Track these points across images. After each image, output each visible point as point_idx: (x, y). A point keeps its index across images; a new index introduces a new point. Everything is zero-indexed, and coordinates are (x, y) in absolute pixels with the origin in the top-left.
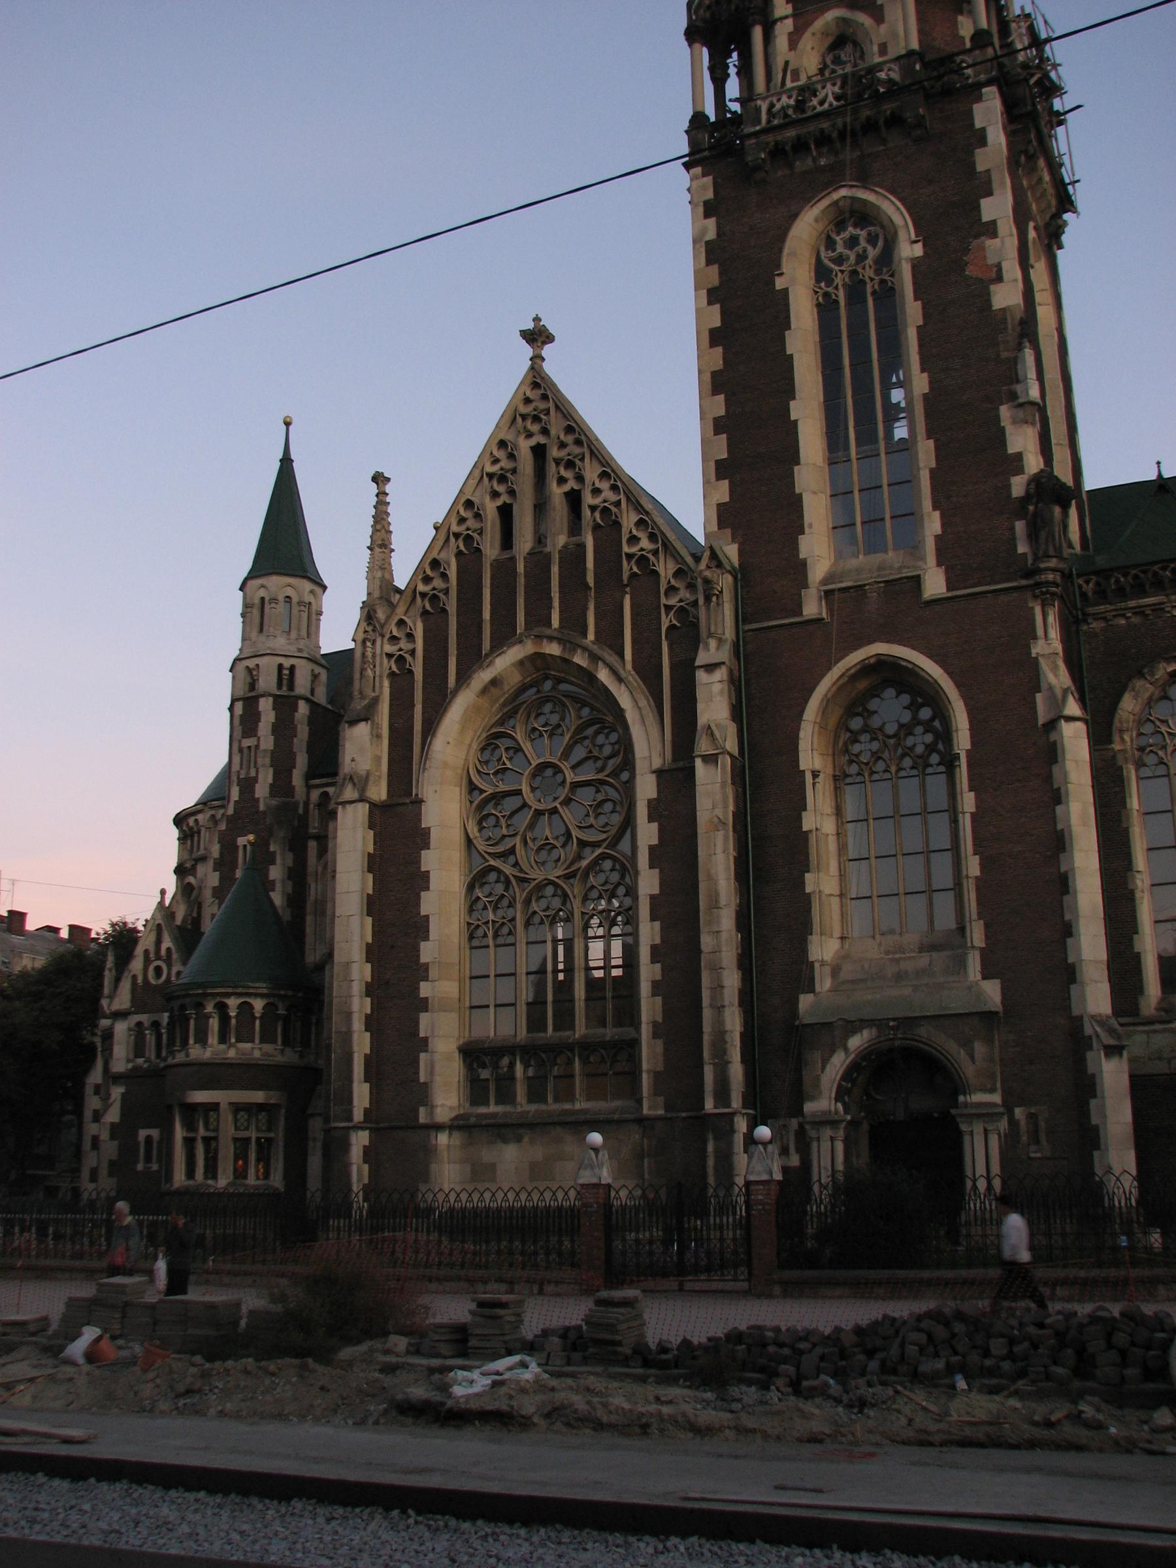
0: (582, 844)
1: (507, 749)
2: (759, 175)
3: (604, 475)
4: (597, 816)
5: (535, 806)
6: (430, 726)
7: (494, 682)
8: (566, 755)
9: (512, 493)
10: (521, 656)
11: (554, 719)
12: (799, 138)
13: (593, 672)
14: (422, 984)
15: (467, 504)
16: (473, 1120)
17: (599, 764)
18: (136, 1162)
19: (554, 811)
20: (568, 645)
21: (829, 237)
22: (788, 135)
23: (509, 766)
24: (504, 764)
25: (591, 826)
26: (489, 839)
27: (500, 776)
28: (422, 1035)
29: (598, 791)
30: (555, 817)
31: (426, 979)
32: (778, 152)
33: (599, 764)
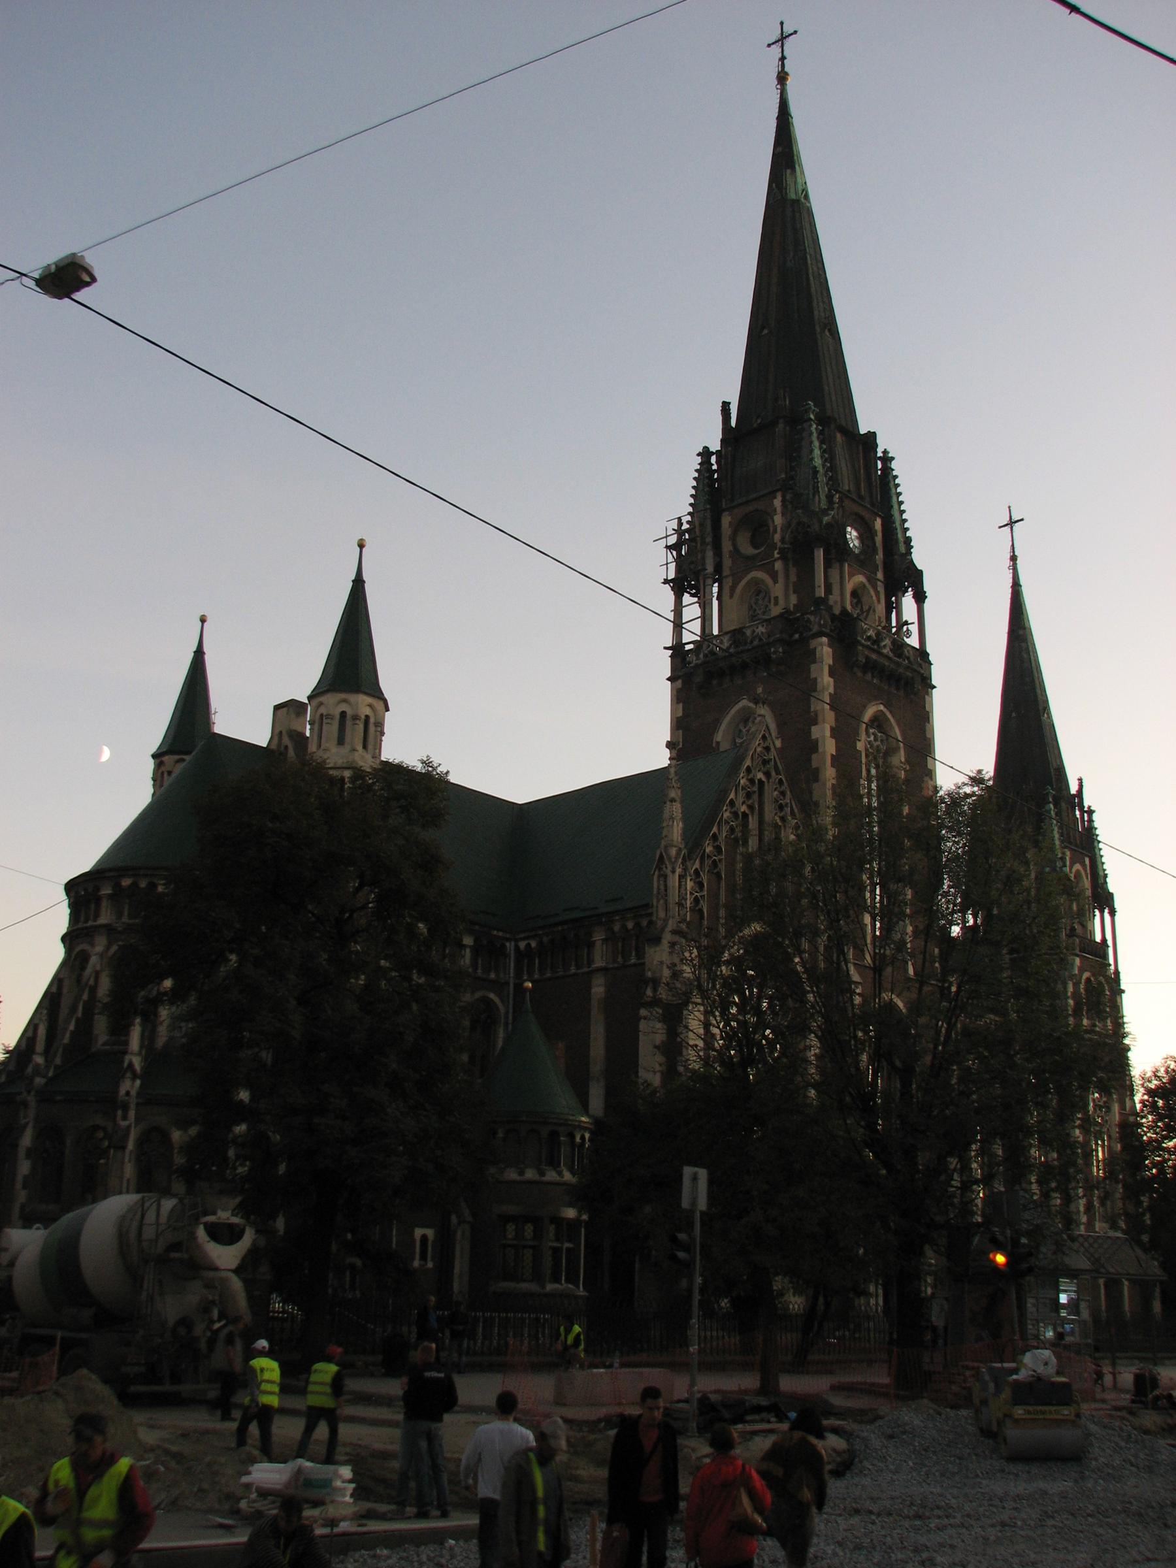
12: (876, 660)
18: (413, 1259)
32: (870, 666)
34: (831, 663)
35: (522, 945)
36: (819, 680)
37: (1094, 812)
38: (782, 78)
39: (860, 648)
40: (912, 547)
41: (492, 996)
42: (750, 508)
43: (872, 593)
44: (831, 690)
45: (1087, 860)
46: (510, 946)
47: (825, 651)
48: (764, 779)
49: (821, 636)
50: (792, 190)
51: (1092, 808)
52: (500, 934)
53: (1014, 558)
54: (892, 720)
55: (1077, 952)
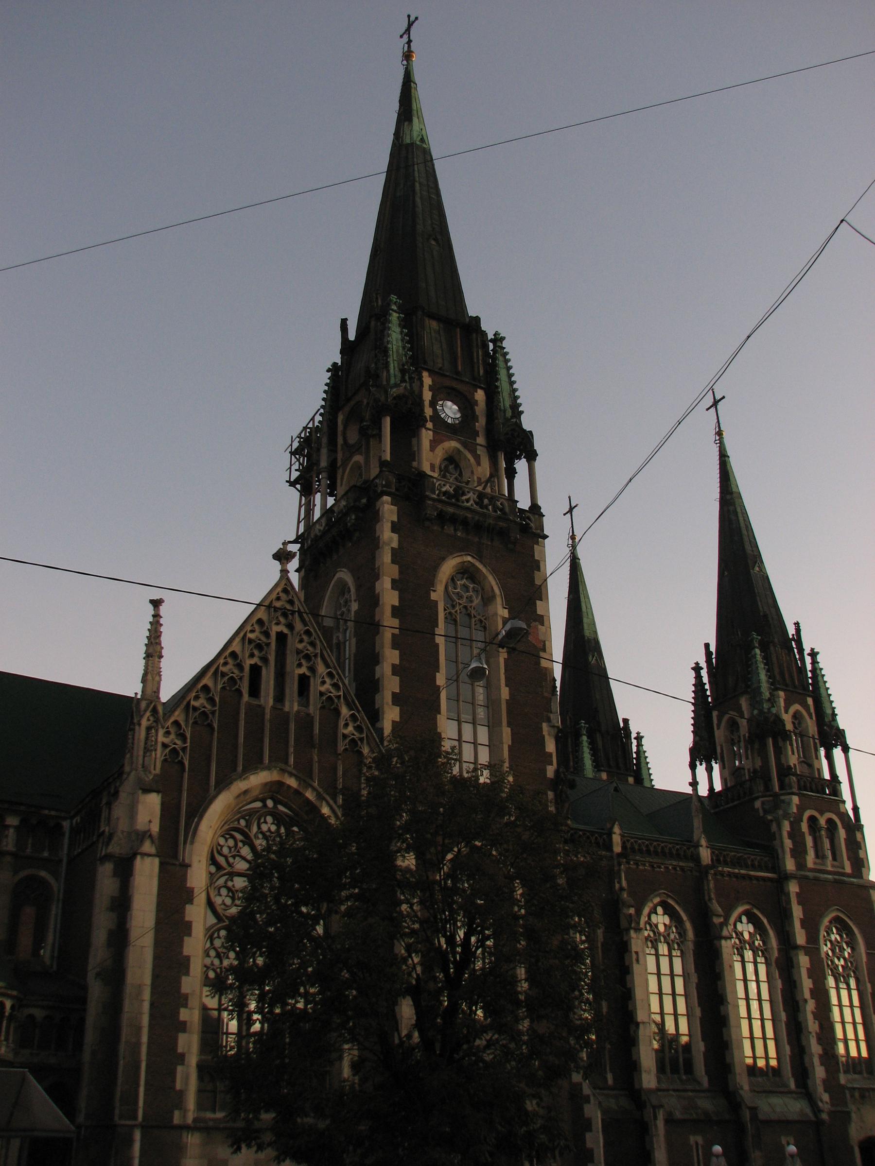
1: (241, 841)
2: (427, 523)
3: (330, 675)
6: (197, 810)
7: (246, 792)
9: (265, 660)
10: (269, 779)
12: (454, 514)
13: (319, 806)
14: (182, 1010)
15: (227, 653)
16: (211, 1124)
20: (302, 782)
21: (453, 579)
22: (450, 510)
28: (180, 1050)
31: (186, 1006)
32: (442, 518)
34: (395, 519)
35: (74, 821)
36: (381, 537)
37: (818, 653)
38: (408, 56)
39: (430, 502)
40: (522, 412)
41: (43, 874)
42: (352, 403)
43: (469, 456)
44: (395, 544)
45: (810, 701)
46: (66, 824)
47: (388, 510)
48: (286, 631)
49: (382, 496)
50: (408, 137)
51: (815, 651)
52: (53, 813)
53: (719, 433)
54: (484, 570)
55: (795, 790)
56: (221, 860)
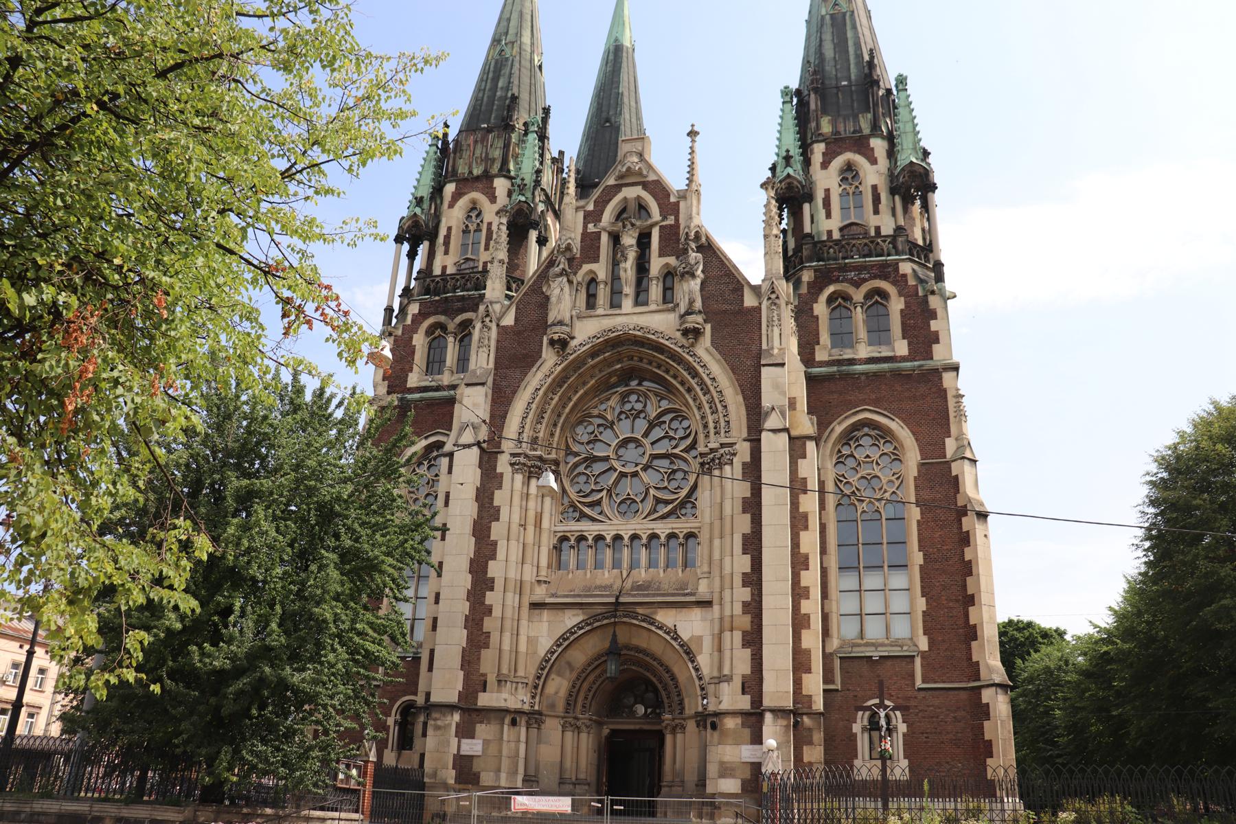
0: (658, 501)
1: (599, 426)
4: (669, 481)
5: (620, 469)
8: (646, 435)
11: (639, 406)
17: (674, 443)
19: (635, 474)
23: (600, 438)
24: (596, 436)
25: (665, 488)
26: (581, 490)
27: (591, 446)
29: (672, 463)
30: (635, 479)
33: (674, 443)
56: (575, 448)
